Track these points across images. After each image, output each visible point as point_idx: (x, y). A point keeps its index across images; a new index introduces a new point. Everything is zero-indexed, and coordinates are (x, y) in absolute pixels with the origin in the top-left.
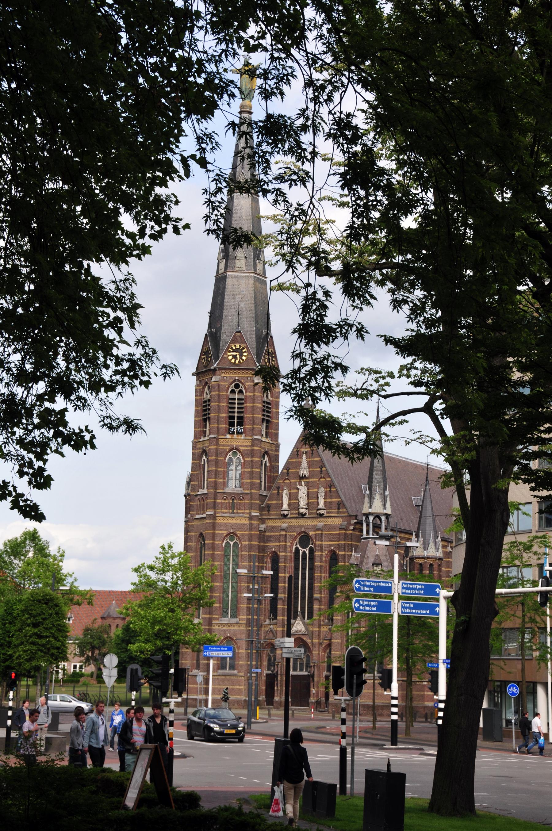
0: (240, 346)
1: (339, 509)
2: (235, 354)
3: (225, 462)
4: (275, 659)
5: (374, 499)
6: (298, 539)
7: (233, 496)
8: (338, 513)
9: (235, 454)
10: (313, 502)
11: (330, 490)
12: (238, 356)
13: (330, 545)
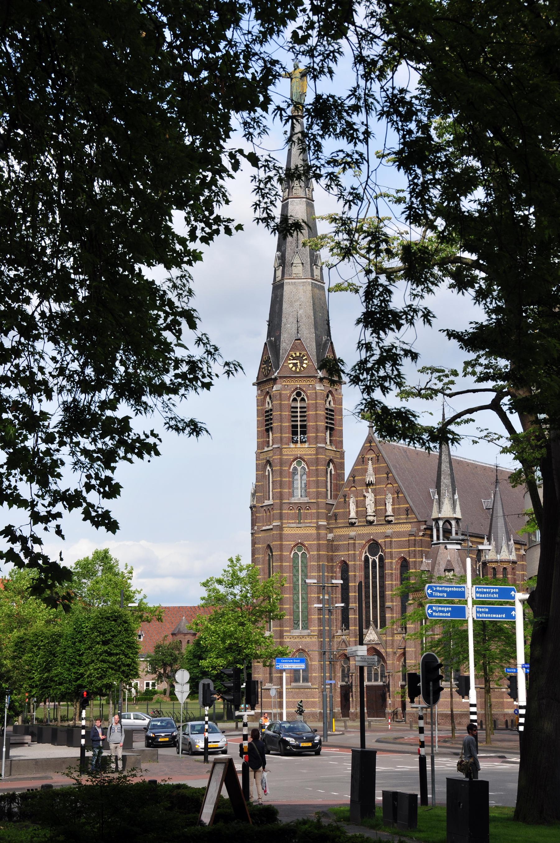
0: (300, 354)
1: (407, 515)
2: (295, 361)
3: (289, 472)
4: (349, 670)
5: (443, 503)
6: (367, 547)
7: (300, 506)
8: (406, 519)
9: (299, 463)
10: (381, 509)
12: (299, 364)
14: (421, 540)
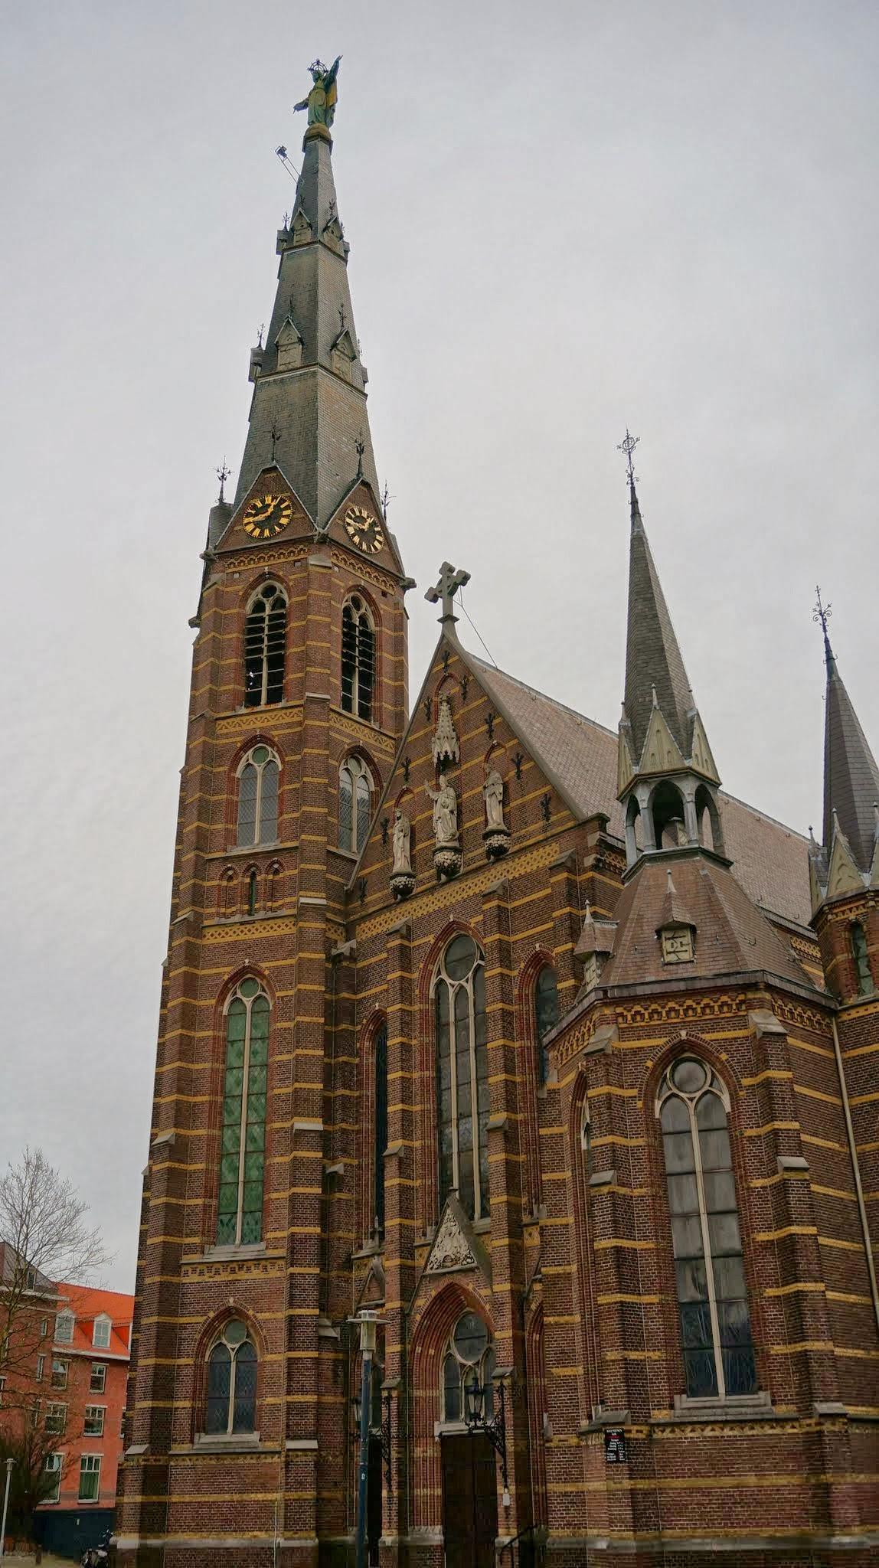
1: (547, 816)
3: (232, 780)
6: (441, 955)
7: (252, 863)
14: (592, 879)
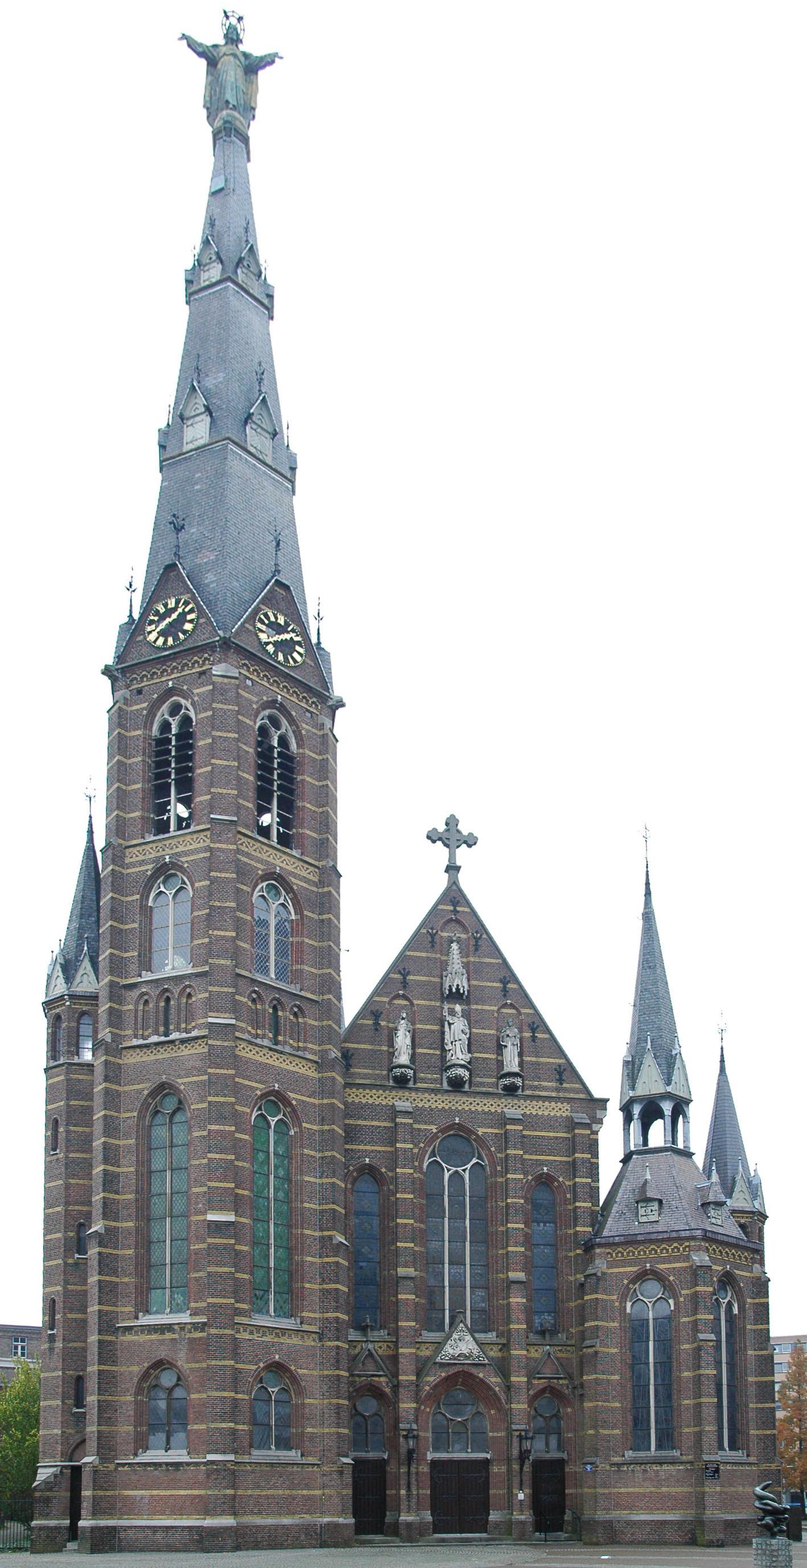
1: (561, 1081)
8: (557, 1090)
11: (534, 1038)
13: (542, 1163)
